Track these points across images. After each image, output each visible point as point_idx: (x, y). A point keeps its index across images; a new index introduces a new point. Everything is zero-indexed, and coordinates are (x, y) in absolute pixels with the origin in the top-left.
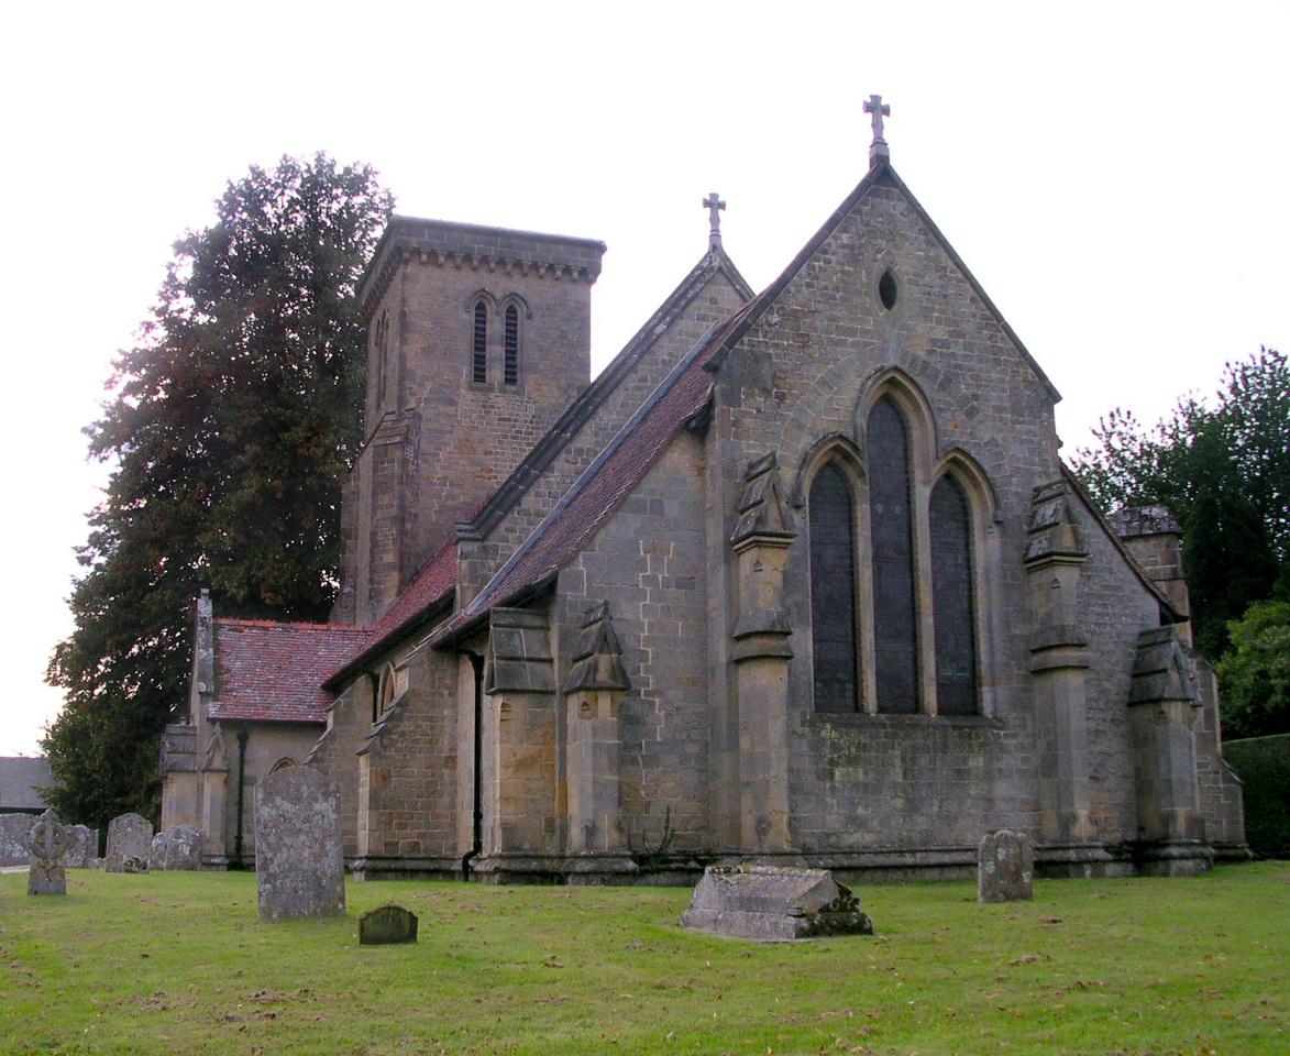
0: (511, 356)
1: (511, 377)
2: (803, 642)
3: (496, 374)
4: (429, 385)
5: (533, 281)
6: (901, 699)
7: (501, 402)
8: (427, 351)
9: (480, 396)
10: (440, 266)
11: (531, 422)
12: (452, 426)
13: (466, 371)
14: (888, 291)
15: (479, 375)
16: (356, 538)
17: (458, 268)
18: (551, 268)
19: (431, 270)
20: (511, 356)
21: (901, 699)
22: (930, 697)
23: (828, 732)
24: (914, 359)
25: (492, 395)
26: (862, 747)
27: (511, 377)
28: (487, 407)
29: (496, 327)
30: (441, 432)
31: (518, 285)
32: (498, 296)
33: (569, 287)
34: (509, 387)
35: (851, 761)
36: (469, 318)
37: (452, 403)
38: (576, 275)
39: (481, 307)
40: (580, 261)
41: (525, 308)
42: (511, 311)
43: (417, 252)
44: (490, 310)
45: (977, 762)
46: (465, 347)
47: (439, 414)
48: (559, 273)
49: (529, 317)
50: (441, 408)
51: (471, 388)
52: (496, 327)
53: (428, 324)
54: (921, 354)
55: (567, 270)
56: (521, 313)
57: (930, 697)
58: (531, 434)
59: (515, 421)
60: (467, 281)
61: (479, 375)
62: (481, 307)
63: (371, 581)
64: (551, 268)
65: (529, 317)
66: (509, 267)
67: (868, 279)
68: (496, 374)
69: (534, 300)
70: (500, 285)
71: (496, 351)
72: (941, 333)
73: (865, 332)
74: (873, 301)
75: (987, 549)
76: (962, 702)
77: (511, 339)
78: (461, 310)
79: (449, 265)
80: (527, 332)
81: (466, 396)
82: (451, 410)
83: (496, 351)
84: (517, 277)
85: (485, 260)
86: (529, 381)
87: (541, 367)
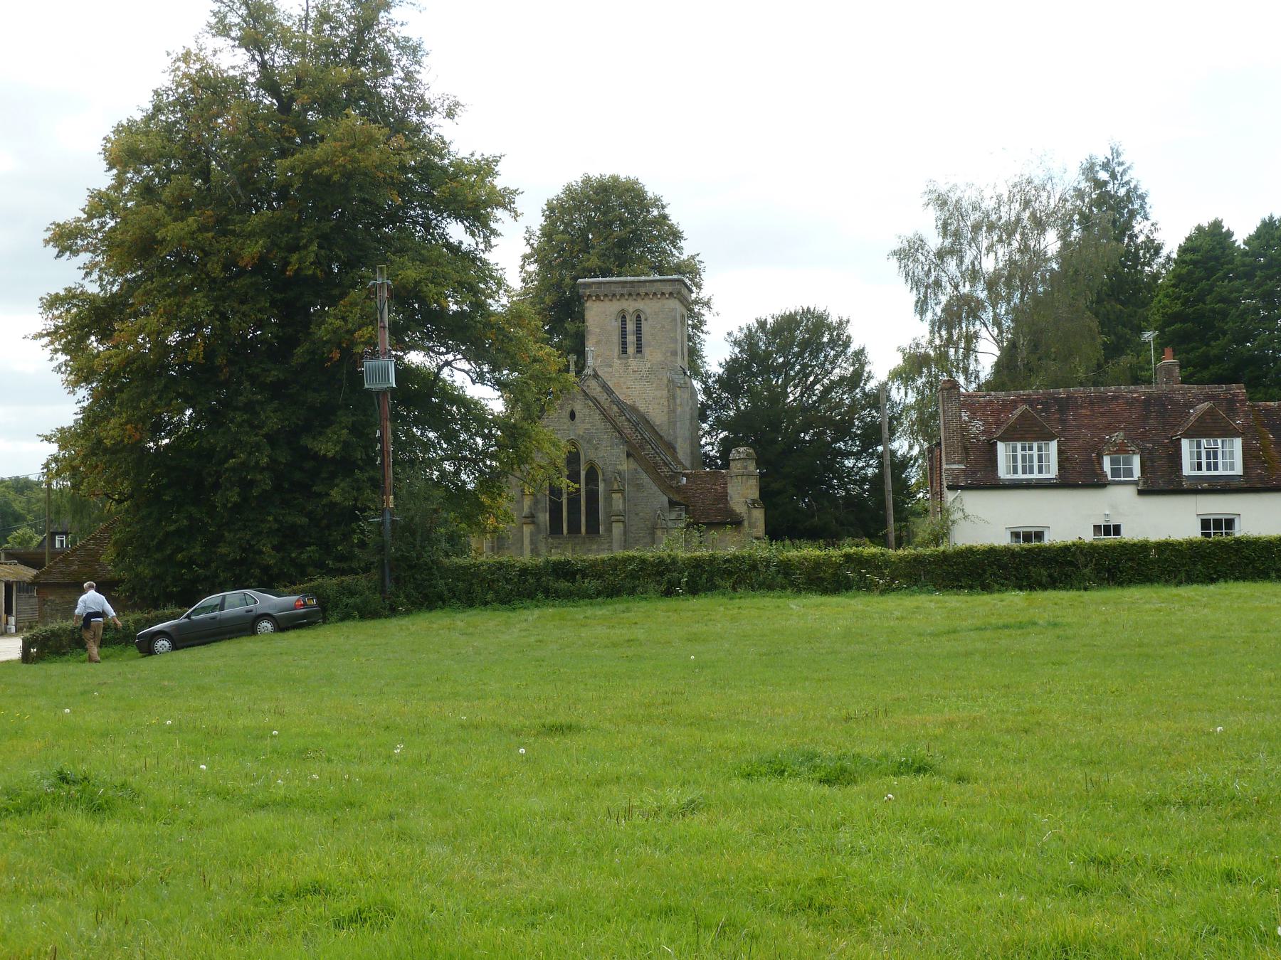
0: (639, 339)
1: (639, 350)
2: (544, 518)
3: (631, 350)
5: (647, 301)
6: (574, 529)
7: (633, 363)
8: (598, 343)
9: (624, 361)
13: (616, 350)
14: (572, 416)
15: (624, 351)
17: (611, 300)
19: (598, 304)
20: (639, 339)
21: (574, 529)
22: (583, 529)
23: (550, 540)
24: (579, 435)
25: (629, 360)
26: (561, 544)
27: (639, 350)
28: (627, 366)
29: (631, 327)
31: (640, 305)
34: (639, 355)
35: (556, 547)
37: (611, 366)
38: (667, 296)
39: (624, 317)
42: (639, 317)
43: (590, 296)
45: (595, 547)
46: (616, 338)
48: (659, 296)
49: (646, 320)
50: (606, 370)
51: (619, 358)
52: (631, 327)
53: (598, 330)
54: (581, 433)
55: (663, 294)
56: (643, 318)
57: (583, 529)
60: (614, 307)
64: (655, 294)
65: (646, 320)
66: (634, 297)
67: (566, 413)
68: (631, 350)
69: (648, 311)
70: (630, 306)
71: (631, 338)
72: (588, 426)
73: (564, 430)
74: (566, 420)
75: (601, 487)
76: (593, 529)
77: (638, 331)
78: (613, 321)
80: (645, 327)
81: (617, 362)
83: (631, 338)
85: (622, 295)
86: (646, 350)
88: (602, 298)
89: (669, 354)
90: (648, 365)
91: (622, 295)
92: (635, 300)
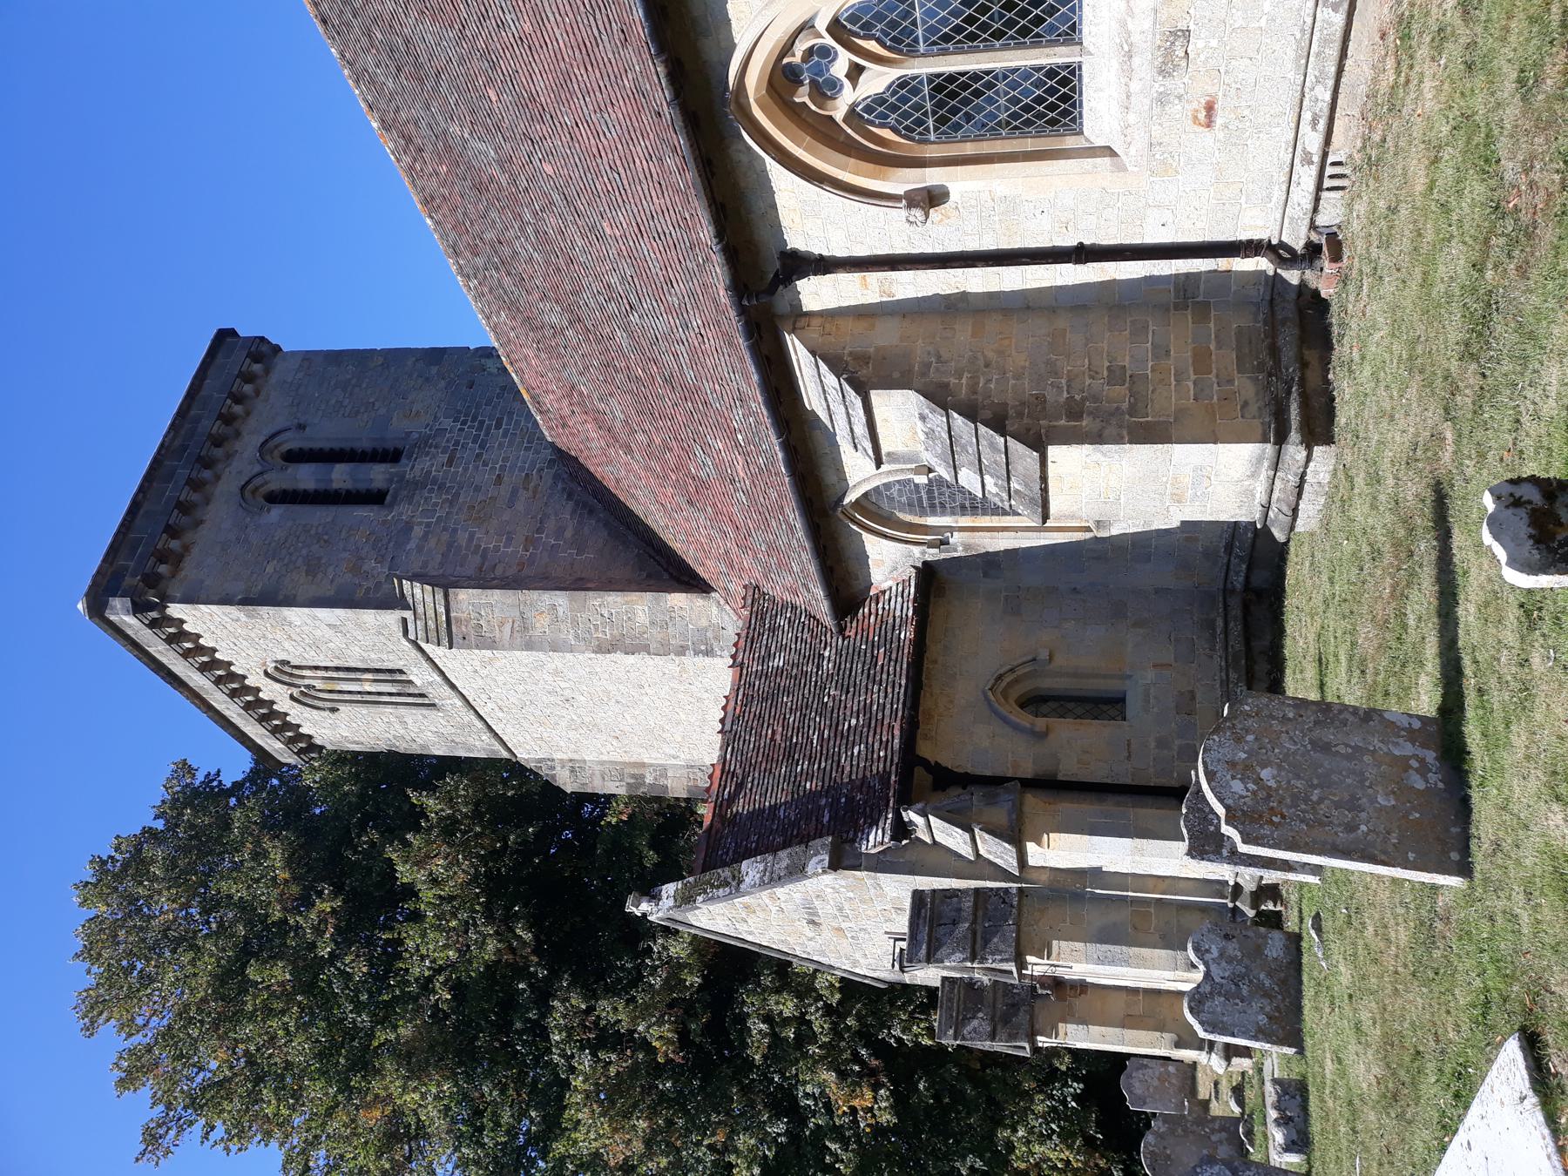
3: (377, 475)
4: (370, 565)
10: (186, 549)
11: (464, 423)
12: (445, 529)
16: (643, 765)
18: (238, 399)
29: (306, 477)
30: (450, 545)
32: (257, 468)
33: (274, 378)
36: (276, 512)
37: (408, 527)
40: (236, 360)
41: (288, 434)
44: (277, 481)
46: (320, 515)
47: (420, 549)
50: (412, 545)
51: (391, 506)
52: (306, 477)
56: (292, 442)
58: (482, 422)
59: (457, 443)
60: (220, 513)
61: (375, 498)
62: (274, 498)
63: (681, 651)
65: (301, 427)
71: (340, 476)
79: (189, 537)
80: (326, 433)
81: (403, 511)
82: (418, 531)
83: (340, 476)
84: (238, 446)
86: (401, 426)
87: (383, 411)
88: (174, 544)
89: (434, 370)
90: (447, 423)
91: (196, 485)
92: (229, 456)
